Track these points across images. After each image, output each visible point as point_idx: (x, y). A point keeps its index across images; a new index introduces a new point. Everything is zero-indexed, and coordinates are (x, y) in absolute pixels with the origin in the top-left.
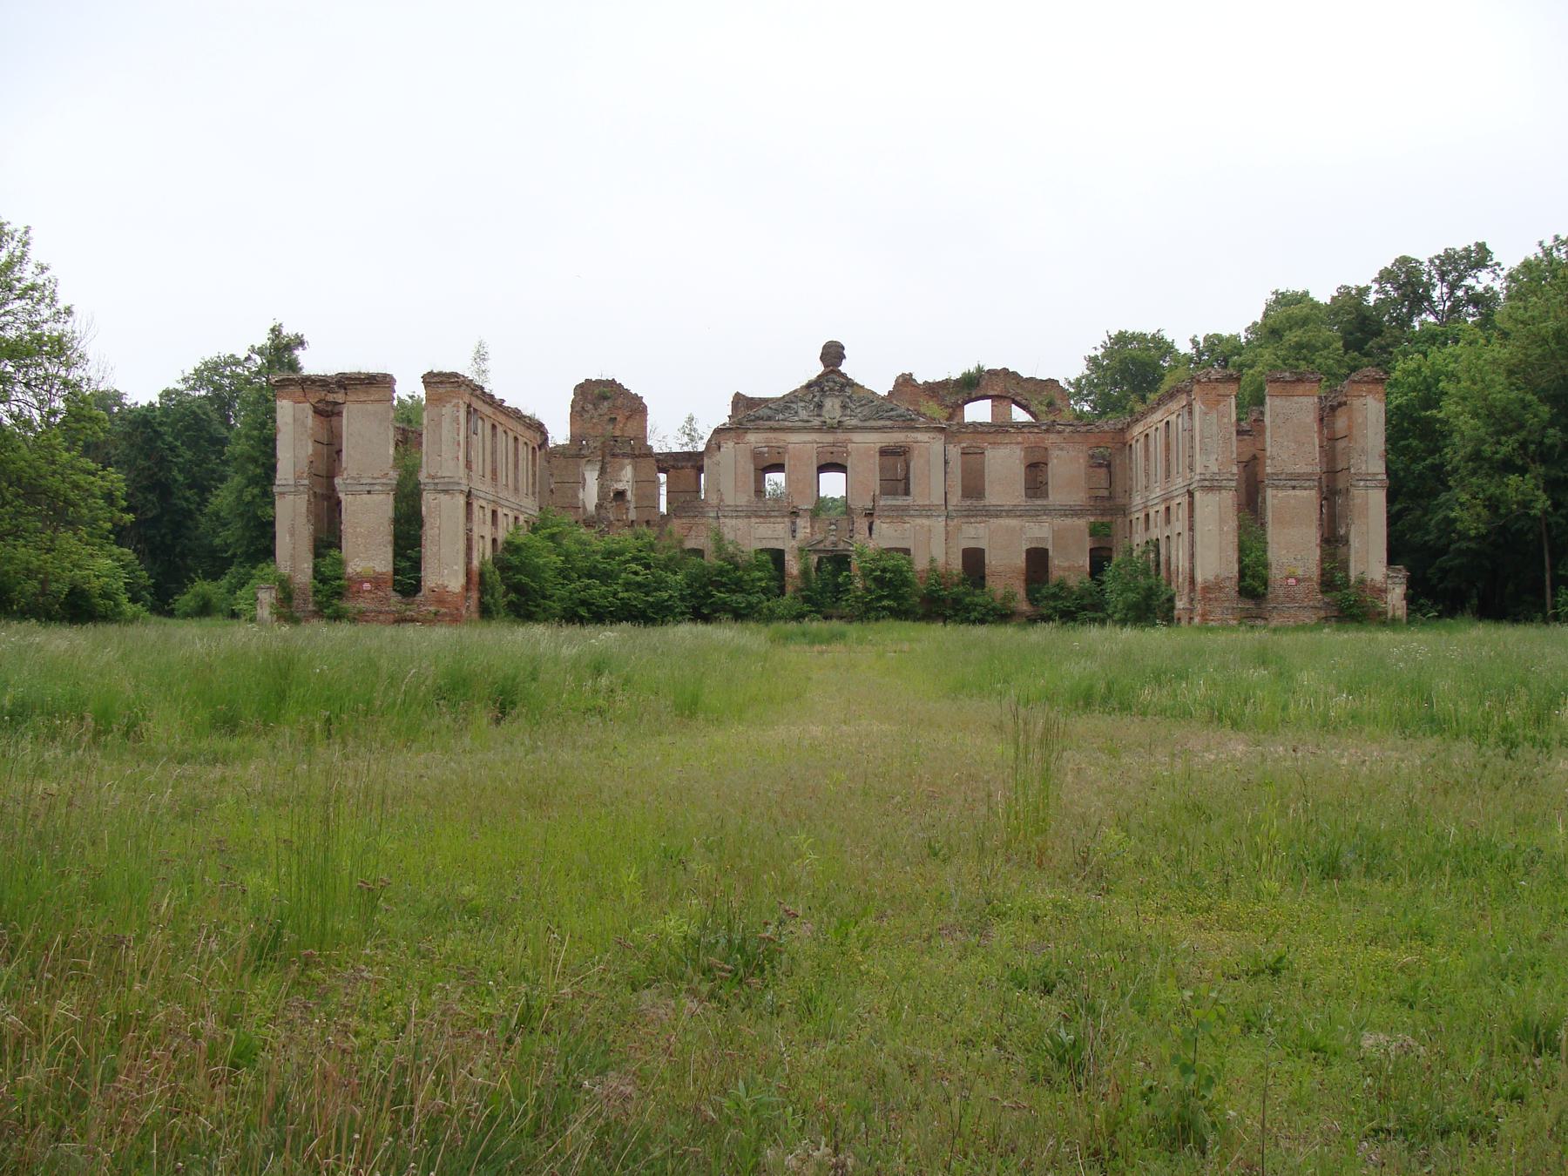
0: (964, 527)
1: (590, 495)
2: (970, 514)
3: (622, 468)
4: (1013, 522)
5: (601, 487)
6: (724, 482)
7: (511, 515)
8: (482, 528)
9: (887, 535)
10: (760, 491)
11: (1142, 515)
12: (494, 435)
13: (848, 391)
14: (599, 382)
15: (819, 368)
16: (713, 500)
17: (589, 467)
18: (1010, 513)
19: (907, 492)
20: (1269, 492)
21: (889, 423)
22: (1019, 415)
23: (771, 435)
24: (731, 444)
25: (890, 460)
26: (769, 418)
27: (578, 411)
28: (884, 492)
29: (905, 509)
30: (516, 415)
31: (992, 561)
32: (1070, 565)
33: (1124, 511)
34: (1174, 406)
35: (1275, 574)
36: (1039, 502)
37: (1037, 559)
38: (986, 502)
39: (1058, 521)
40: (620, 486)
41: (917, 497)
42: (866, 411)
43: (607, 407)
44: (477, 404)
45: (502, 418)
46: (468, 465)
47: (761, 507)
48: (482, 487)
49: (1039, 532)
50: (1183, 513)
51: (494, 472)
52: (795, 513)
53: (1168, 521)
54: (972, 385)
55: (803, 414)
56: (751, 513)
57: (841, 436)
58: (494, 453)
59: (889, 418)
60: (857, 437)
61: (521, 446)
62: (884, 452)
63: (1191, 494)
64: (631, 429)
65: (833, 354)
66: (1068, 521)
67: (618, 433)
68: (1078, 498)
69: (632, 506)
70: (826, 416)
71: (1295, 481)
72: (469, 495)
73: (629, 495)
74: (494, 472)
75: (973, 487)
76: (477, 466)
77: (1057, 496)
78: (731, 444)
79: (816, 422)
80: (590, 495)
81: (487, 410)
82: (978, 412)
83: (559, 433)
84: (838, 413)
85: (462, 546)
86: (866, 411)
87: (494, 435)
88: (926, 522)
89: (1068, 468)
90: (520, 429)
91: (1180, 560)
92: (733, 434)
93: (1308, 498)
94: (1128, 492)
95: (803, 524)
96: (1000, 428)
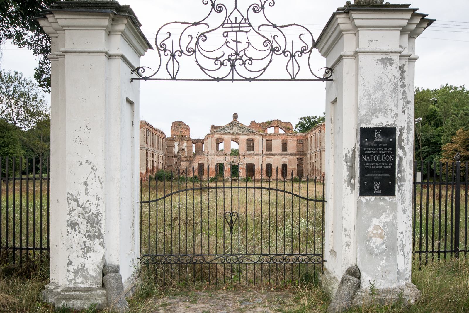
0: (267, 158)
1: (176, 150)
2: (268, 155)
3: (184, 143)
4: (279, 157)
5: (179, 148)
6: (209, 146)
7: (157, 155)
8: (150, 158)
9: (249, 160)
10: (217, 149)
11: (310, 156)
12: (153, 135)
13: (239, 125)
14: (178, 122)
15: (232, 120)
16: (206, 151)
17: (176, 143)
19: (253, 150)
21: (249, 133)
22: (281, 131)
23: (220, 136)
24: (210, 138)
25: (249, 142)
26: (220, 132)
27: (173, 129)
28: (247, 150)
29: (252, 154)
30: (159, 131)
31: (274, 167)
32: (293, 167)
33: (306, 155)
34: (317, 130)
36: (285, 152)
37: (285, 166)
38: (272, 152)
39: (290, 157)
40: (183, 148)
41: (256, 151)
42: (243, 130)
43: (180, 127)
44: (149, 128)
45: (155, 131)
46: (147, 143)
47: (218, 152)
48: (150, 148)
49: (285, 160)
50: (318, 156)
51: (153, 144)
52: (226, 155)
53: (315, 158)
54: (269, 124)
55: (228, 131)
56: (215, 155)
57: (237, 136)
58: (153, 139)
59: (249, 132)
60: (241, 136)
61: (159, 138)
62: (247, 140)
63: (321, 151)
64: (186, 133)
65: (235, 116)
66: (292, 157)
67: (183, 134)
68: (295, 151)
69: (186, 152)
70: (234, 131)
72: (147, 150)
73: (186, 150)
74: (153, 144)
75: (269, 148)
76: (149, 143)
77: (289, 151)
78: (210, 138)
79: (231, 133)
80: (176, 150)
81: (151, 129)
82: (271, 130)
83: (168, 135)
84: (236, 130)
85: (145, 162)
86: (243, 130)
87: (153, 135)
88: (257, 157)
89: (292, 144)
90: (159, 134)
91: (318, 167)
92: (211, 135)
94: (307, 150)
95: (228, 157)
96: (276, 135)
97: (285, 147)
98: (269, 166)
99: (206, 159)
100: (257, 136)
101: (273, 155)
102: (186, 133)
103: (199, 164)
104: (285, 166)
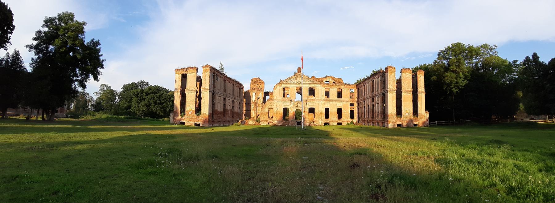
2: (327, 100)
7: (231, 100)
9: (310, 105)
18: (335, 101)
20: (403, 94)
35: (403, 112)
37: (340, 111)
39: (344, 103)
44: (216, 73)
49: (340, 105)
66: (346, 103)
71: (407, 91)
75: (327, 94)
77: (343, 98)
90: (235, 83)
93: (410, 95)
97: (340, 95)
98: (327, 110)
99: (275, 105)
100: (317, 85)
101: (330, 101)
102: (261, 86)
103: (173, 92)
104: (340, 111)
